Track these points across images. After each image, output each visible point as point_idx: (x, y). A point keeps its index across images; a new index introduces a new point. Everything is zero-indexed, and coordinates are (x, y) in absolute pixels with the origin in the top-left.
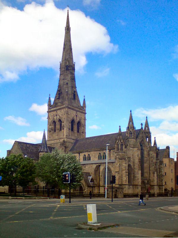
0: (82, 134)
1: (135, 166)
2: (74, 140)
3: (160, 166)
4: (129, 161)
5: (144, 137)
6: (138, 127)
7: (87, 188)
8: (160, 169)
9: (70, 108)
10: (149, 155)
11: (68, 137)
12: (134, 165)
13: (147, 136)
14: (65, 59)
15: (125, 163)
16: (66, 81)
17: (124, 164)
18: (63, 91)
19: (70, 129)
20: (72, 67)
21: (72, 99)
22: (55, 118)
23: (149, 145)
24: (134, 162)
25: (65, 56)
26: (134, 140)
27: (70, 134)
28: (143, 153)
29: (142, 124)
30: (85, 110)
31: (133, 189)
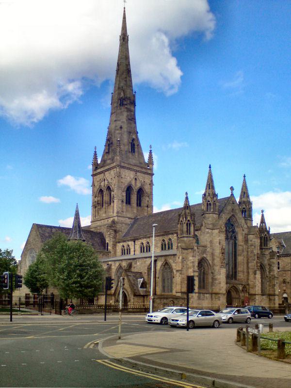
0: (146, 208)
1: (215, 261)
2: (131, 219)
4: (204, 252)
5: (237, 211)
6: (222, 193)
7: (132, 297)
9: (123, 167)
11: (120, 215)
12: (213, 260)
13: (244, 208)
14: (119, 88)
15: (192, 255)
16: (119, 123)
17: (191, 258)
18: (114, 140)
19: (125, 201)
20: (130, 100)
21: (129, 152)
22: (102, 184)
23: (246, 224)
24: (213, 254)
25: (118, 83)
26: (214, 215)
27: (125, 210)
28: (235, 238)
29: (232, 189)
30: (151, 169)
31: (212, 300)
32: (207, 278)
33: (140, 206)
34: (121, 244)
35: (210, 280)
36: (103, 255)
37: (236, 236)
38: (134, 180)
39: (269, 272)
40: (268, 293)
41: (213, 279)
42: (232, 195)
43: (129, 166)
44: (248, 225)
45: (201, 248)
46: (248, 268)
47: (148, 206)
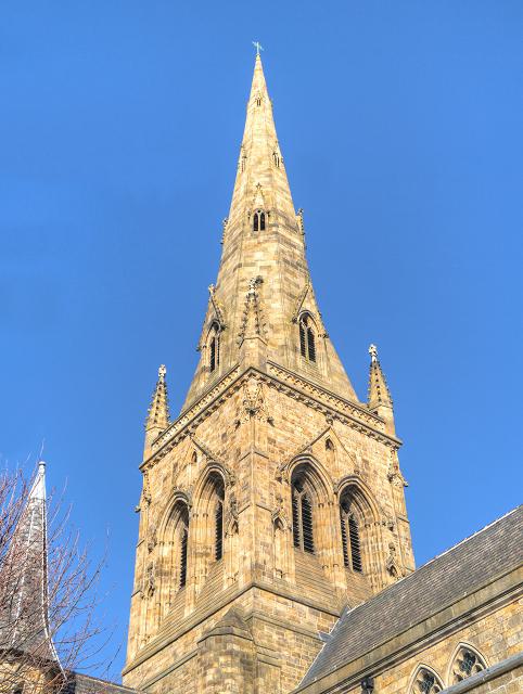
19: (287, 522)
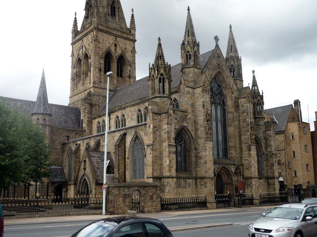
1: (199, 132)
3: (267, 132)
8: (266, 139)
9: (101, 31)
10: (237, 106)
11: (96, 85)
12: (196, 130)
15: (166, 122)
21: (109, 15)
23: (236, 85)
24: (195, 122)
28: (223, 102)
32: (189, 156)
33: (121, 76)
34: (97, 120)
35: (194, 159)
36: (76, 134)
37: (225, 101)
38: (113, 45)
39: (266, 148)
40: (265, 175)
41: (196, 157)
42: (217, 46)
43: (108, 30)
44: (238, 86)
45: (180, 114)
46: (241, 142)
47: (130, 77)
